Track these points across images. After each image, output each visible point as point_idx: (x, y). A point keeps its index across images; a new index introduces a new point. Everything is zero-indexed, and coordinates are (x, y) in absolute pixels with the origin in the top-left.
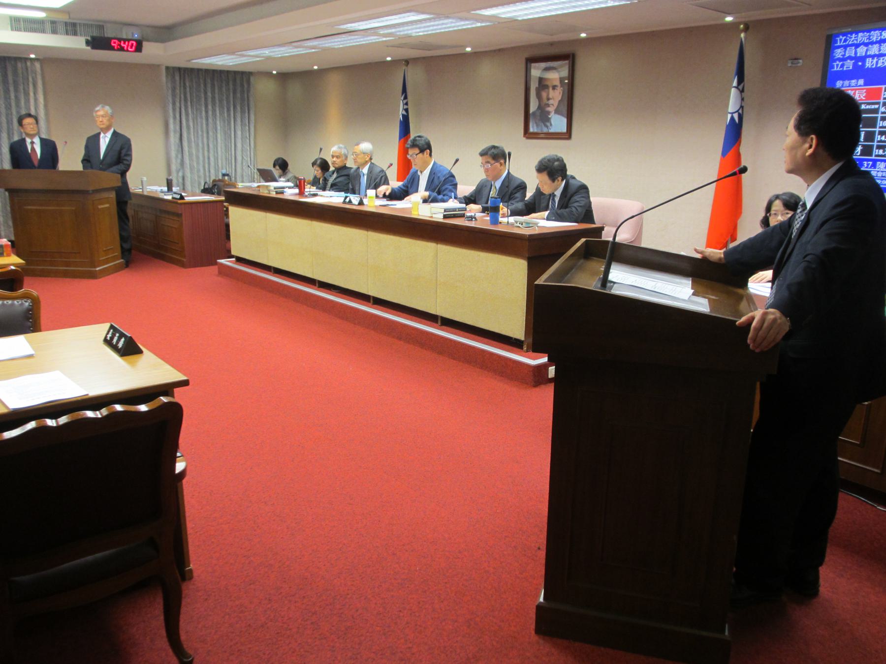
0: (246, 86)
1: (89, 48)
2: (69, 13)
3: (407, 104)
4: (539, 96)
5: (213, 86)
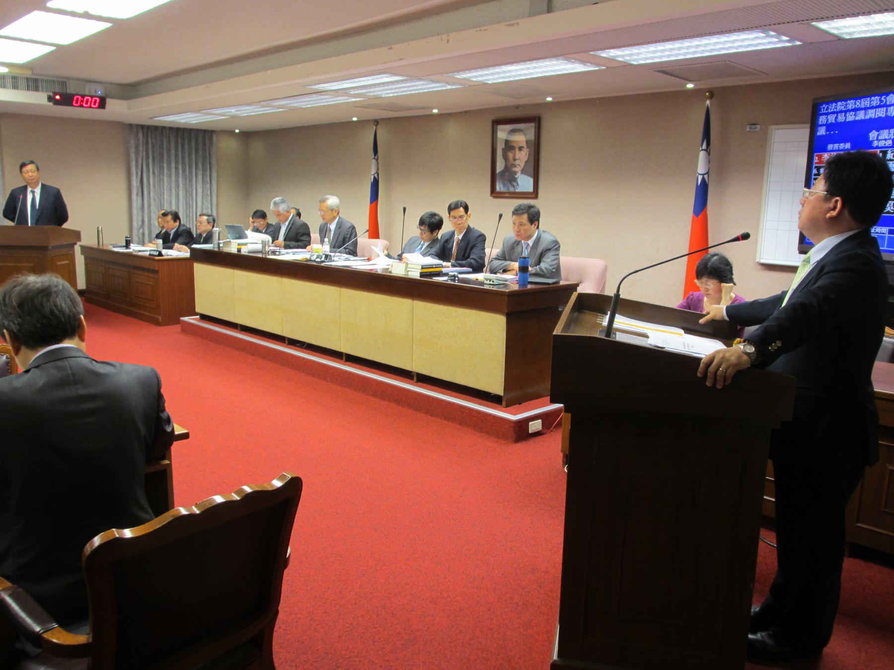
0: (207, 143)
1: (51, 104)
2: (32, 69)
4: (505, 157)
5: (176, 143)
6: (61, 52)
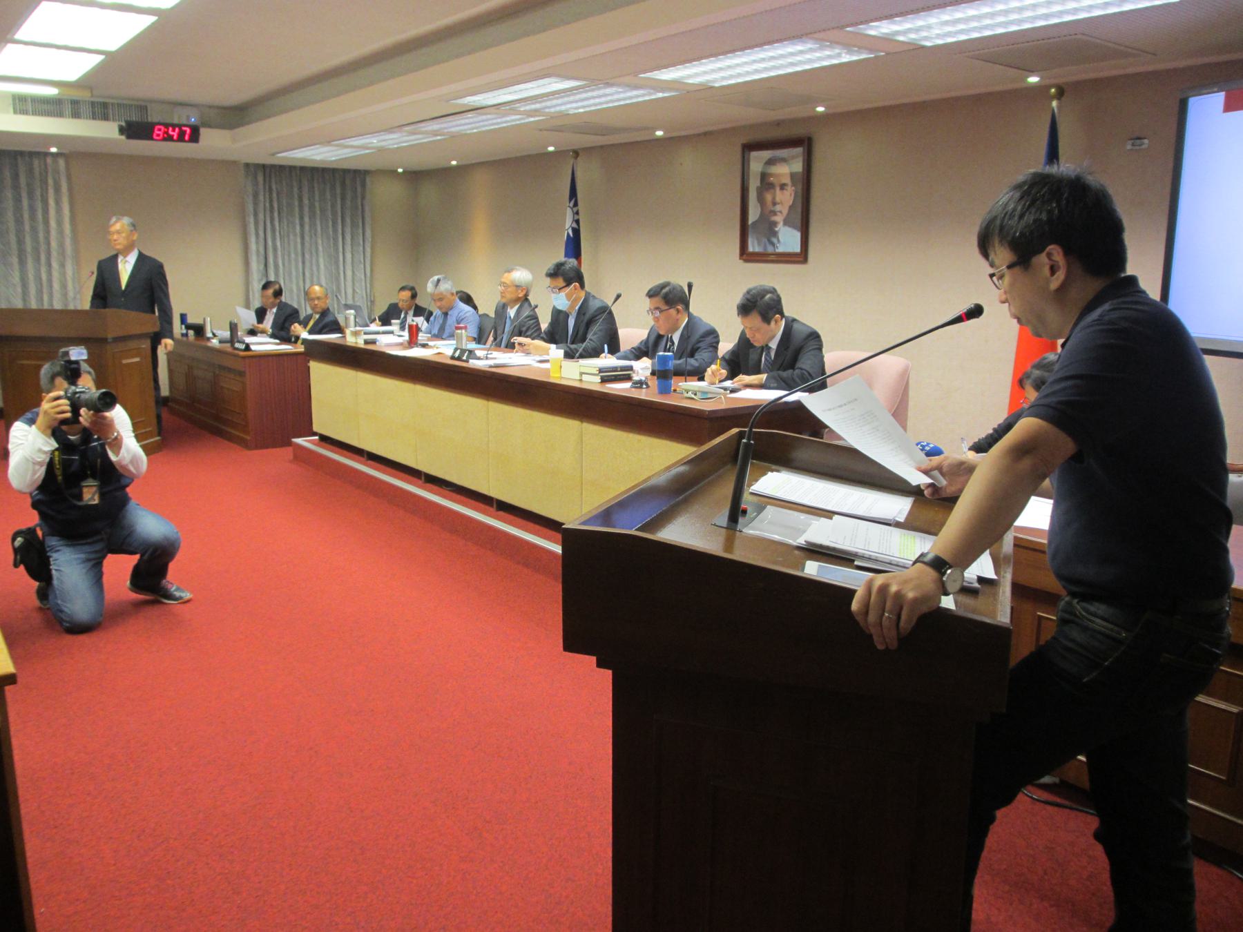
0: (359, 189)
1: (123, 137)
2: (91, 89)
3: (577, 213)
5: (311, 189)
6: (114, 62)
